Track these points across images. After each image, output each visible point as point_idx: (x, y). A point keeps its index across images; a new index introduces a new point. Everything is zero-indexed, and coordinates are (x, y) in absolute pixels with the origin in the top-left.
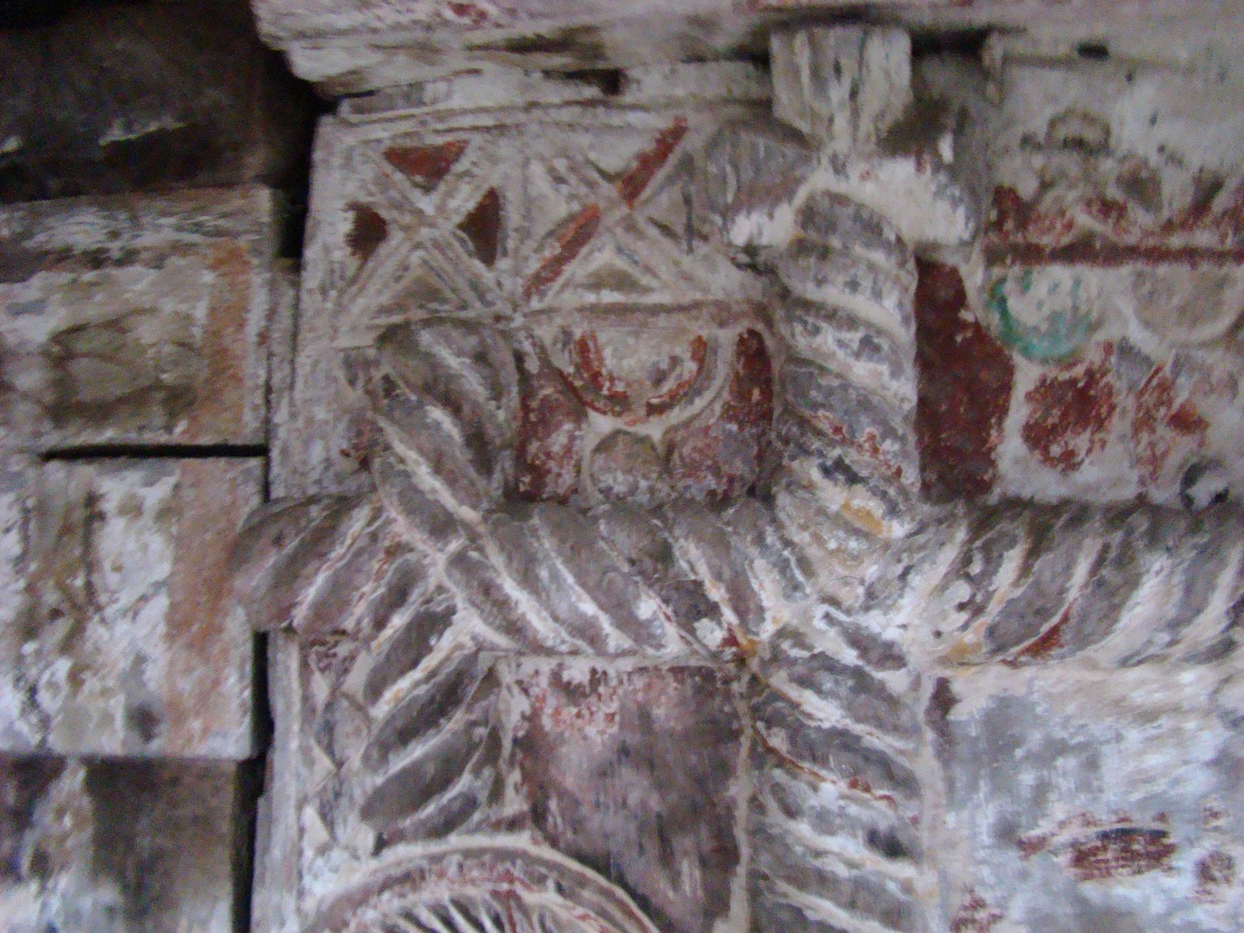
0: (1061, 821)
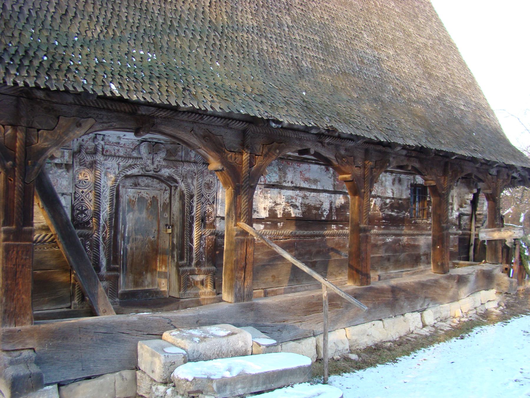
0: (106, 167)
